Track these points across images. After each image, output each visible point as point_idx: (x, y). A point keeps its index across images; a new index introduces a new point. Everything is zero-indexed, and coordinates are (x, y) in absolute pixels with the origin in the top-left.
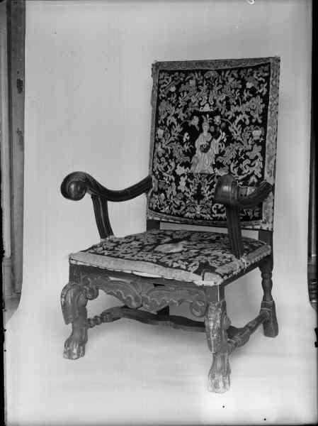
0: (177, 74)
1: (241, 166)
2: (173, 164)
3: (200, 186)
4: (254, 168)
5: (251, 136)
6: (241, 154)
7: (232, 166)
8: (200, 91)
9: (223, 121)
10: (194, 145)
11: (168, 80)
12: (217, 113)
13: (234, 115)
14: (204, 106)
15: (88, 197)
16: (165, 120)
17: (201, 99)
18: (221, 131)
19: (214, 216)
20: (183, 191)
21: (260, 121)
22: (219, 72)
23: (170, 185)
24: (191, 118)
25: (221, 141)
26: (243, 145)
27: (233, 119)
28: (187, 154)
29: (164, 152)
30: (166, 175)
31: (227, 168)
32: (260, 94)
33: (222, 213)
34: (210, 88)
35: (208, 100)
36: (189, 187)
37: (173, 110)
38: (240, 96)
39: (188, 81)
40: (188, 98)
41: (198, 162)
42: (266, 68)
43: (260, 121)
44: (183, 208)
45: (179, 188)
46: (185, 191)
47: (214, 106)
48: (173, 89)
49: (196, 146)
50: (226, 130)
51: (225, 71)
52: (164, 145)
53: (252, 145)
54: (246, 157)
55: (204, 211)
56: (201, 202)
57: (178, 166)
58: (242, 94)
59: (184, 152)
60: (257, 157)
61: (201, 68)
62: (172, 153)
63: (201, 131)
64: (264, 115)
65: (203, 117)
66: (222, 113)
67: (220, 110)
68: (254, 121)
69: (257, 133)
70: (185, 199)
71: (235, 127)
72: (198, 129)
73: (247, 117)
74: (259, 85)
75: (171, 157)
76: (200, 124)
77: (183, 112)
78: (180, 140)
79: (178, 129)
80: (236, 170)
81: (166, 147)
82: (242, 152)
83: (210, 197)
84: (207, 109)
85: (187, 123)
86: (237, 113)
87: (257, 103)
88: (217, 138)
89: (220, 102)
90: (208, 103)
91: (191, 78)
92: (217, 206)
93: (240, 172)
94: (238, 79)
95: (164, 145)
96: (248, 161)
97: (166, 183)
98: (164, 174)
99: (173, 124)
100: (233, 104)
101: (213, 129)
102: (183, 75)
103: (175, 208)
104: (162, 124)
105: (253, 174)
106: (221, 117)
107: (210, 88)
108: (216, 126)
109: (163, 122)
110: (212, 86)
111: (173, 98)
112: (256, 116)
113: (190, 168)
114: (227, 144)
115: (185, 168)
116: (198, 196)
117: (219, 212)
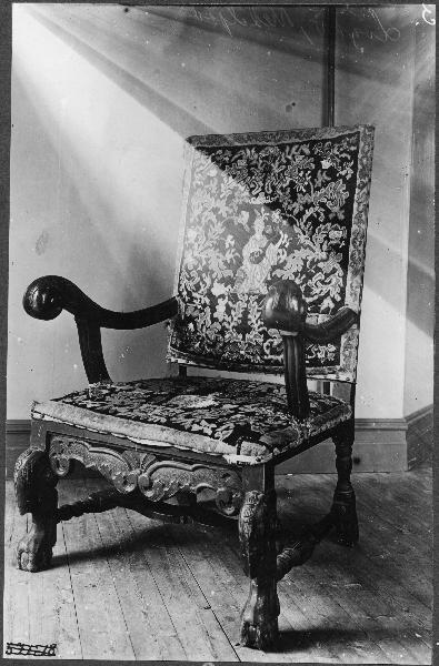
0: (220, 152)
1: (310, 282)
3: (246, 312)
4: (330, 287)
5: (327, 238)
10: (241, 253)
13: (302, 208)
15: (66, 319)
17: (252, 186)
21: (341, 217)
22: (282, 148)
23: (201, 311)
24: (239, 213)
25: (282, 246)
26: (314, 251)
27: (300, 215)
28: (228, 265)
30: (198, 296)
32: (343, 177)
33: (279, 354)
35: (263, 188)
36: (229, 315)
38: (312, 180)
39: (236, 161)
43: (341, 217)
46: (224, 320)
47: (272, 195)
49: (244, 255)
51: (291, 145)
53: (329, 252)
57: (215, 284)
58: (314, 175)
59: (225, 262)
60: (334, 271)
63: (253, 232)
64: (348, 207)
68: (331, 216)
72: (247, 229)
76: (251, 223)
79: (219, 228)
82: (313, 263)
85: (232, 221)
86: (307, 206)
91: (241, 158)
95: (196, 254)
96: (320, 276)
97: (196, 308)
98: (194, 295)
100: (301, 192)
103: (209, 346)
105: (328, 294)
106: (283, 211)
108: (274, 225)
110: (271, 167)
114: (290, 251)
117: (273, 352)
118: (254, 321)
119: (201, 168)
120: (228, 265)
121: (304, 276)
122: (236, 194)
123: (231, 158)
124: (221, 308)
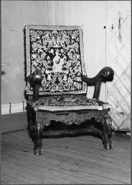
0: (39, 31)
2: (44, 69)
3: (57, 78)
5: (76, 57)
6: (73, 64)
7: (70, 69)
8: (52, 39)
9: (64, 51)
10: (52, 61)
11: (35, 33)
12: (61, 48)
13: (69, 49)
14: (55, 45)
16: (37, 51)
17: (53, 42)
18: (64, 55)
19: (64, 90)
20: (50, 80)
21: (78, 52)
24: (50, 50)
25: (65, 59)
27: (69, 51)
28: (49, 65)
29: (38, 64)
31: (68, 70)
33: (67, 88)
34: (56, 38)
35: (56, 43)
37: (41, 47)
38: (70, 41)
39: (45, 34)
40: (47, 42)
41: (55, 68)
42: (78, 31)
43: (78, 52)
44: (50, 88)
45: (48, 79)
46: (51, 81)
47: (60, 45)
48: (39, 38)
50: (66, 55)
51: (61, 31)
52: (37, 62)
53: (77, 61)
54: (75, 65)
55: (60, 88)
56: (58, 84)
57: (46, 70)
58: (71, 41)
59: (48, 64)
60: (79, 66)
61: (50, 29)
62: (42, 65)
63: (55, 55)
64: (79, 49)
65: (56, 49)
66: (64, 48)
67: (63, 47)
68: (76, 51)
69: (78, 56)
70: (51, 84)
71: (70, 53)
72: (54, 54)
73: (74, 50)
74: (76, 38)
75: (42, 66)
76: (55, 51)
77: (46, 47)
78: (46, 59)
80: (72, 71)
81: (39, 62)
82: (74, 64)
83: (63, 82)
84: (57, 46)
86: (70, 48)
87: (76, 45)
88: (62, 58)
89: (62, 43)
90: (57, 43)
91: (46, 33)
92: (66, 86)
93: (74, 71)
94: (68, 34)
95: (37, 62)
96: (76, 67)
99: (41, 52)
101: (60, 54)
102: (42, 32)
104: (35, 52)
105: (79, 72)
106: (64, 49)
107: (56, 38)
108: (61, 53)
109: (36, 52)
111: (40, 41)
112: (77, 50)
113: (52, 71)
114: (67, 60)
115: (50, 71)
116: (57, 82)
118: (60, 80)
119: (34, 36)
120: (49, 65)
121: (72, 67)
122: (49, 44)
123: (43, 33)
124: (49, 78)
